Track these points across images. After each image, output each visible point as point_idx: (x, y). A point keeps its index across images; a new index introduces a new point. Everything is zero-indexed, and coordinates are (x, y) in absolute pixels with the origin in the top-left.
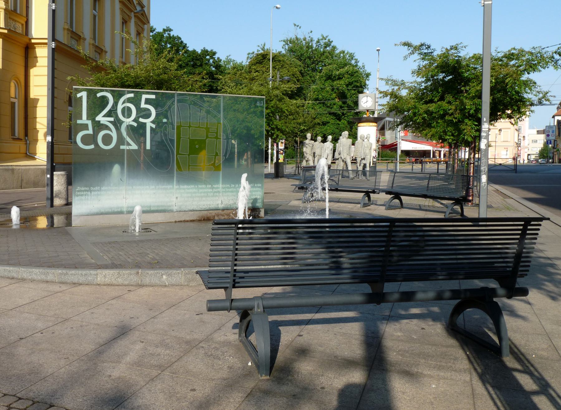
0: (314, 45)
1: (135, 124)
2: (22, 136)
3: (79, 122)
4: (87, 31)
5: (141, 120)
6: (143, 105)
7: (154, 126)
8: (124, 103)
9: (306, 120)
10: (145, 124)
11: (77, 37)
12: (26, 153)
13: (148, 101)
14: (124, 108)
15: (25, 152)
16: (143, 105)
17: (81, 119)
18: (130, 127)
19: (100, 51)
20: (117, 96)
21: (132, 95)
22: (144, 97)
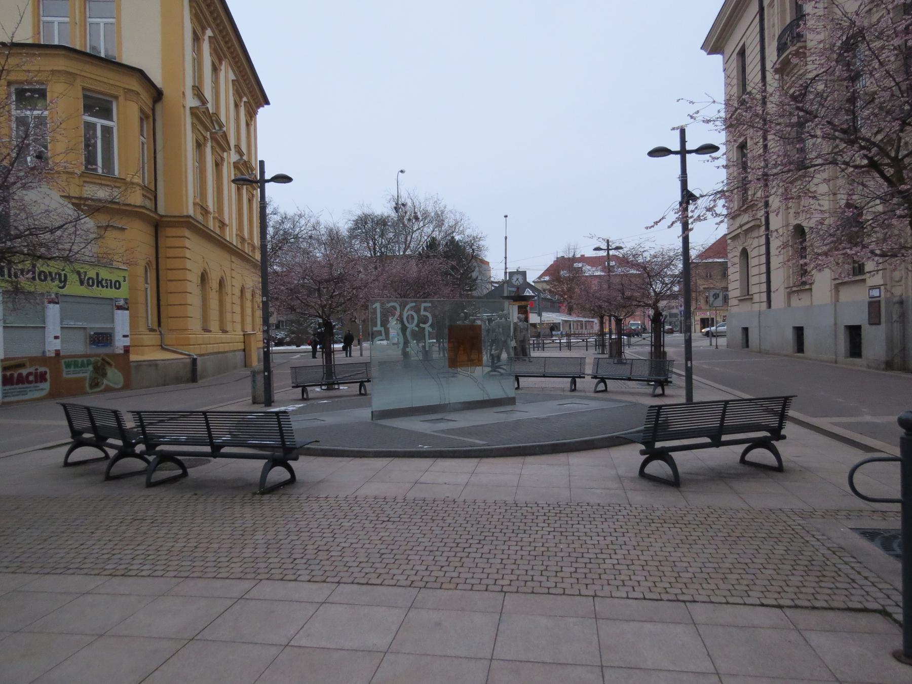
0: (680, 213)
1: (417, 329)
2: (155, 327)
3: (375, 329)
4: (211, 204)
5: (422, 325)
6: (422, 313)
7: (431, 330)
8: (408, 310)
9: (587, 306)
10: (424, 328)
11: (205, 212)
12: (161, 346)
13: (425, 309)
14: (408, 315)
15: (159, 344)
16: (422, 313)
17: (376, 326)
18: (413, 332)
19: (223, 225)
20: (403, 306)
21: (413, 304)
22: (423, 305)
